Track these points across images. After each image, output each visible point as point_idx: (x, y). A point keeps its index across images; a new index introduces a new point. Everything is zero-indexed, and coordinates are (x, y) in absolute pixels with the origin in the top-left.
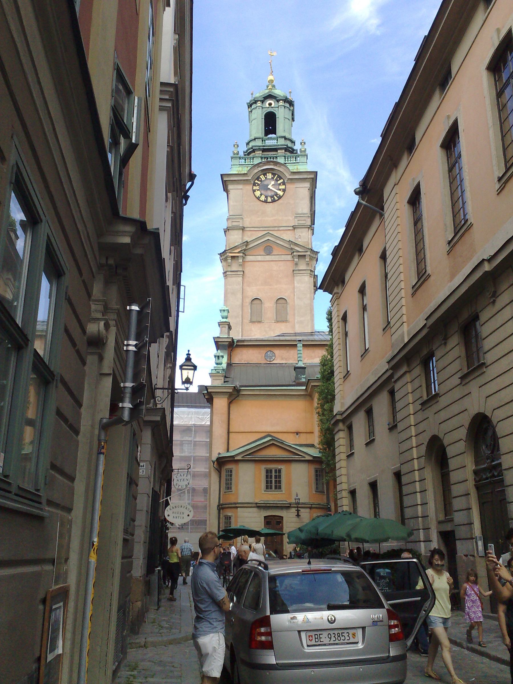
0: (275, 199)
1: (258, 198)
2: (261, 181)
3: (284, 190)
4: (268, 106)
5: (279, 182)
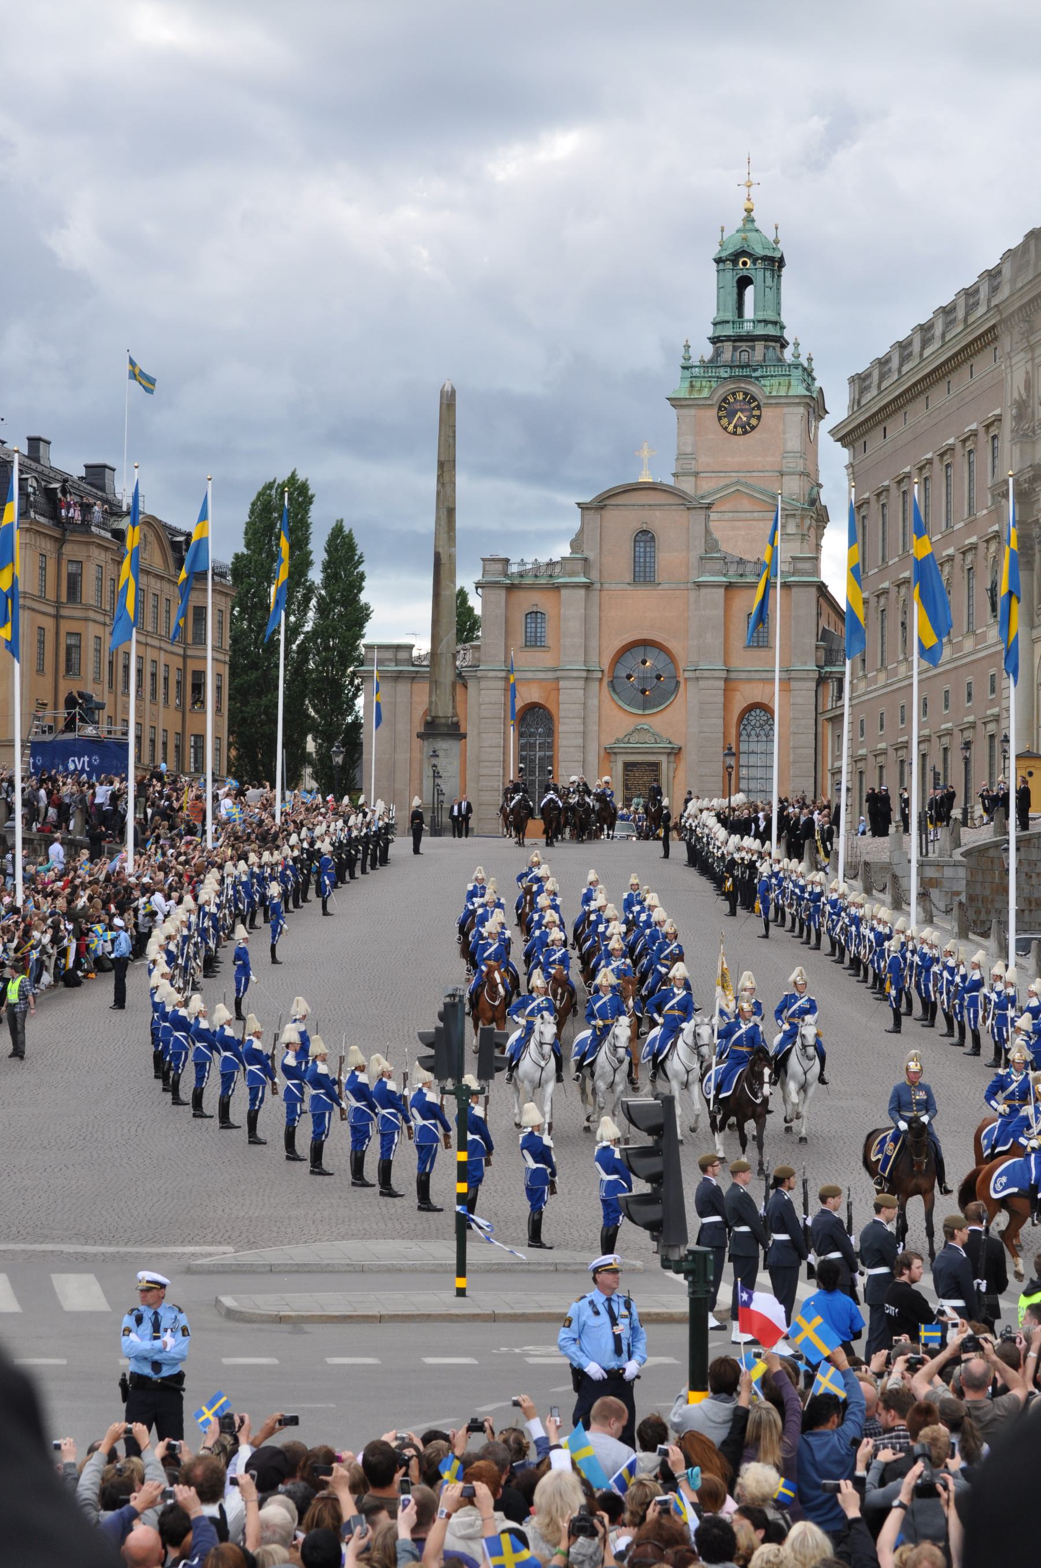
0: (747, 429)
1: (725, 429)
2: (729, 403)
3: (759, 418)
4: (741, 266)
5: (753, 405)
